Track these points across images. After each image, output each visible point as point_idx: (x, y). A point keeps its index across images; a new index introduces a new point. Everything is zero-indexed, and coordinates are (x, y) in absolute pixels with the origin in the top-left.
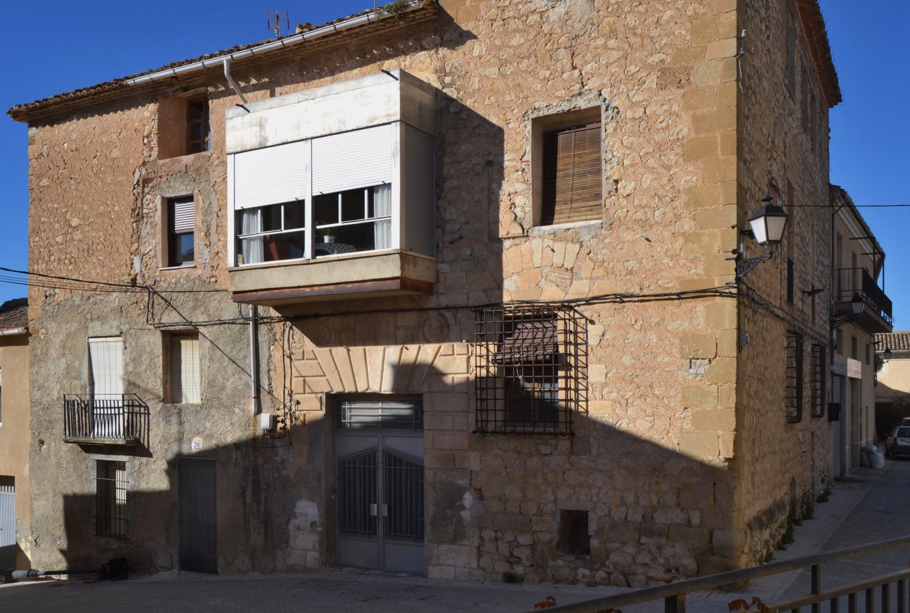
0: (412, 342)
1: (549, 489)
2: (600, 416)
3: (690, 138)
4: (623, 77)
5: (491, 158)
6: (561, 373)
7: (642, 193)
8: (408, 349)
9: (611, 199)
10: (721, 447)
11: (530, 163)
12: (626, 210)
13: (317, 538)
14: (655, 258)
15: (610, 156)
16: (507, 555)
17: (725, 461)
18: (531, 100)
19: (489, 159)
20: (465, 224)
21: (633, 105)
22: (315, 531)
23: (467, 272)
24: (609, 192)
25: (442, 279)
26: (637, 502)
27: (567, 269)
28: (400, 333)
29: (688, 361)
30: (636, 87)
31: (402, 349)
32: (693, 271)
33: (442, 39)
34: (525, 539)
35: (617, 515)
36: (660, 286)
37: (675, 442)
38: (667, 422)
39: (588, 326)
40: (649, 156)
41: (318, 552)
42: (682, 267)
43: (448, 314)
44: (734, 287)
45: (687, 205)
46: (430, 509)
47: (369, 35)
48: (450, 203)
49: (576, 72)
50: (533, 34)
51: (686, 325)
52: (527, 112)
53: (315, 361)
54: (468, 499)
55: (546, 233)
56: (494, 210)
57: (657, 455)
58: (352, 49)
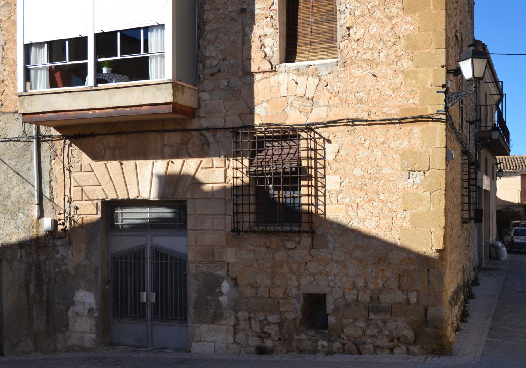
0: (177, 157)
1: (294, 277)
2: (336, 217)
5: (245, 6)
6: (303, 183)
7: (369, 38)
8: (173, 163)
9: (344, 43)
10: (433, 240)
11: (278, 12)
12: (356, 51)
13: (94, 323)
14: (381, 90)
15: (344, 8)
16: (259, 331)
17: (437, 252)
19: (243, 7)
20: (223, 60)
22: (92, 316)
23: (224, 100)
24: (343, 37)
25: (203, 105)
26: (366, 286)
27: (308, 99)
28: (167, 150)
29: (407, 172)
31: (168, 163)
32: (411, 101)
34: (273, 318)
35: (350, 297)
36: (384, 113)
37: (397, 237)
38: (390, 222)
39: (325, 144)
40: (376, 9)
41: (94, 334)
42: (402, 98)
43: (208, 134)
44: (444, 114)
45: (406, 48)
46: (192, 295)
48: (209, 43)
51: (405, 144)
53: (92, 173)
54: (226, 286)
55: (291, 69)
56: (247, 49)
57: (382, 248)
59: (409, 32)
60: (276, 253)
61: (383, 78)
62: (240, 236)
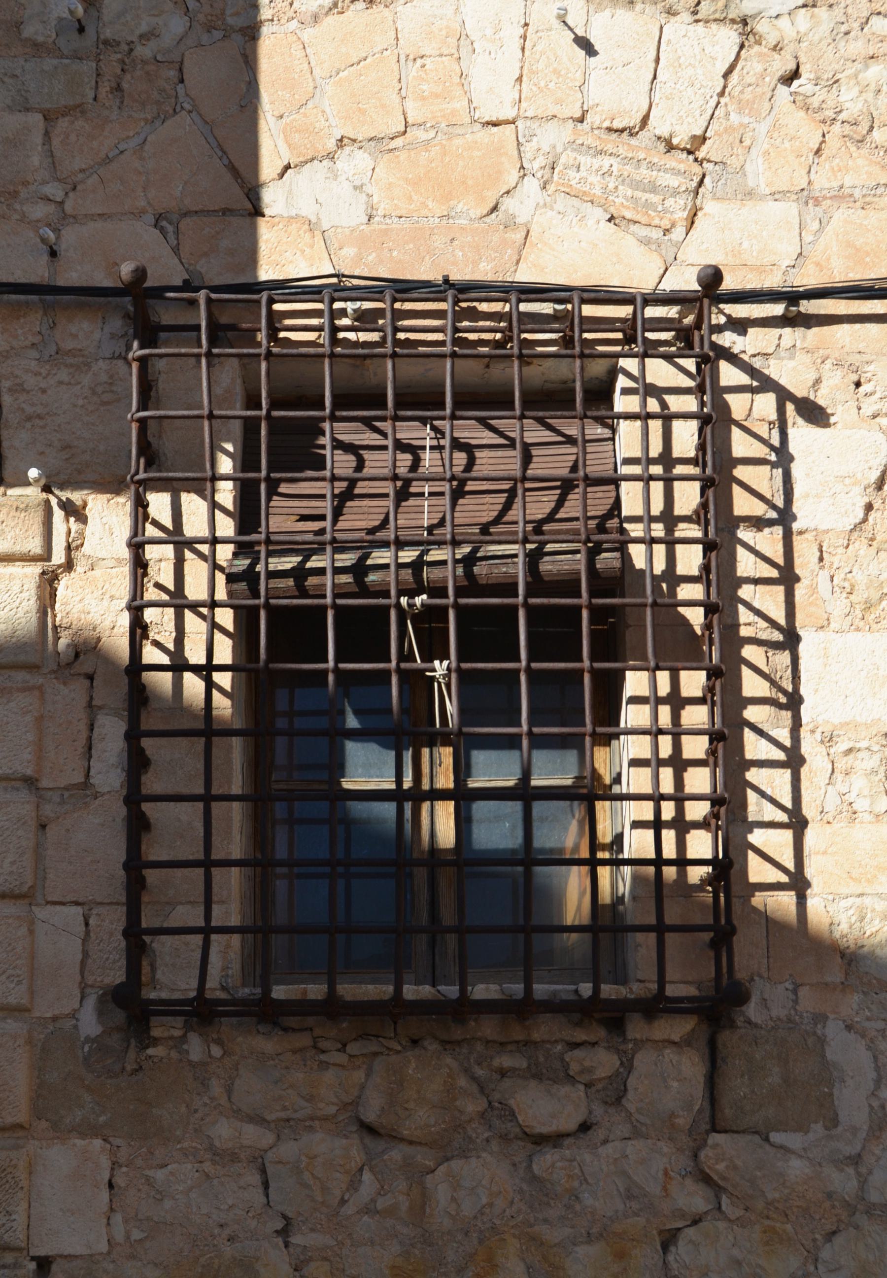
23: (49, 117)
39: (791, 432)
60: (442, 1169)
62: (150, 1051)
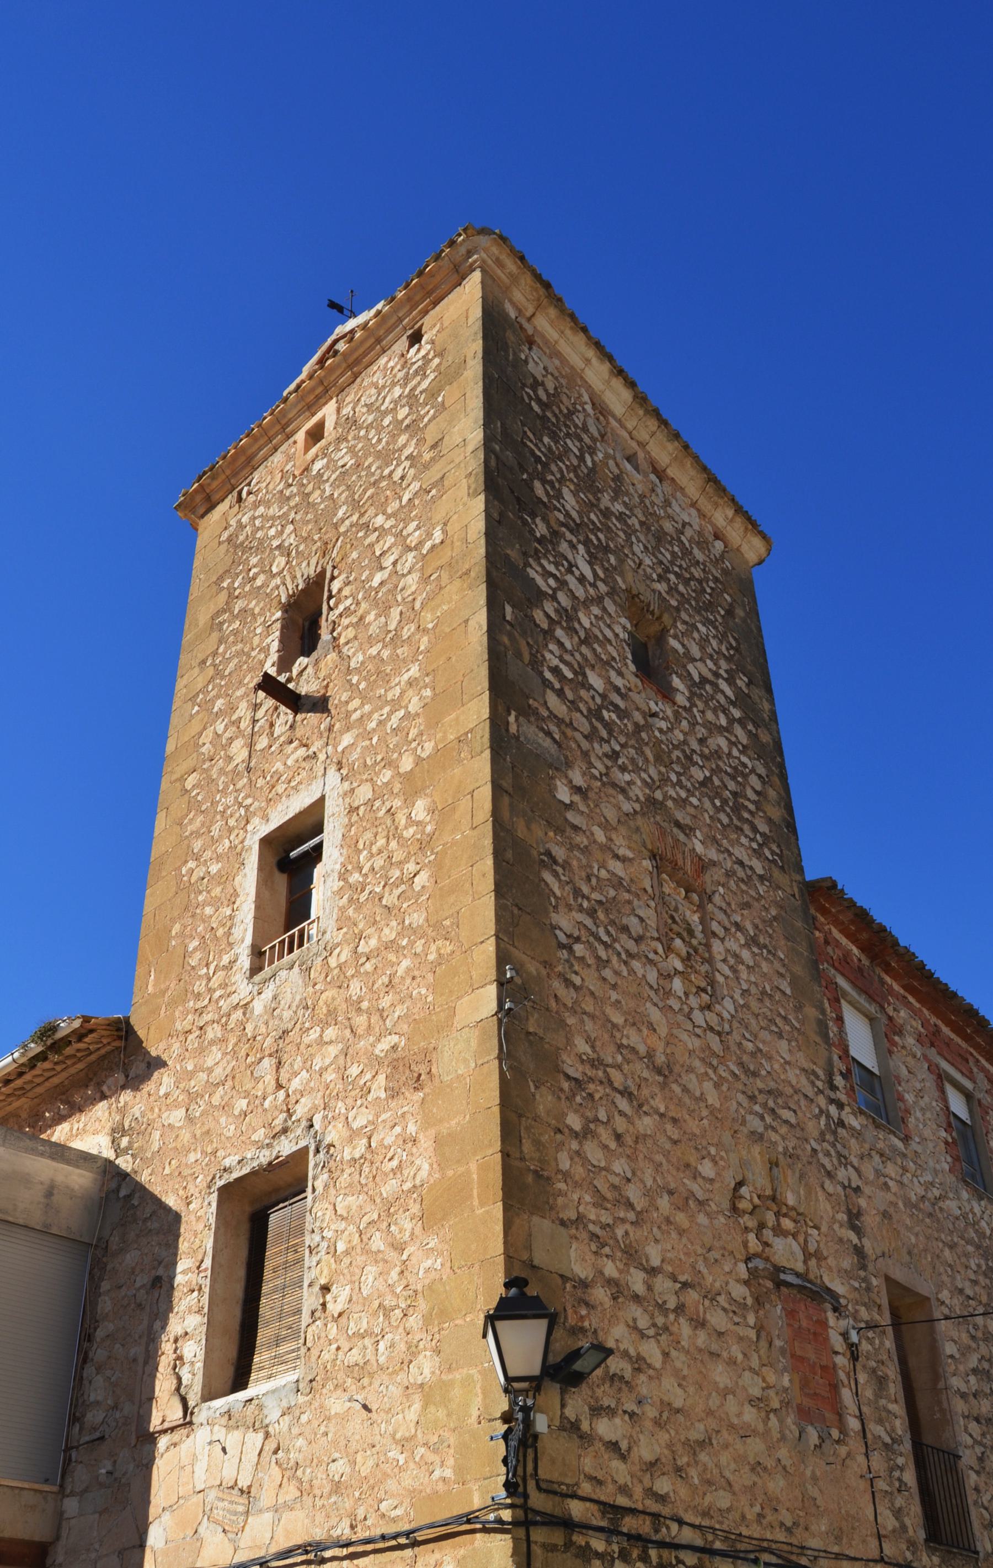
3: (432, 1181)
4: (341, 1086)
5: (160, 1272)
9: (313, 1327)
12: (334, 1346)
15: (317, 1238)
18: (221, 1153)
20: (113, 1409)
21: (354, 1135)
23: (101, 1514)
24: (313, 1313)
25: (64, 1534)
27: (242, 1491)
30: (359, 1102)
32: (437, 1474)
33: (127, 1076)
45: (427, 1320)
47: (40, 1090)
48: (99, 1370)
49: (281, 1094)
50: (233, 1041)
52: (214, 1178)
56: (149, 1375)
58: (24, 1115)
59: (433, 1275)
61: (382, 1414)
